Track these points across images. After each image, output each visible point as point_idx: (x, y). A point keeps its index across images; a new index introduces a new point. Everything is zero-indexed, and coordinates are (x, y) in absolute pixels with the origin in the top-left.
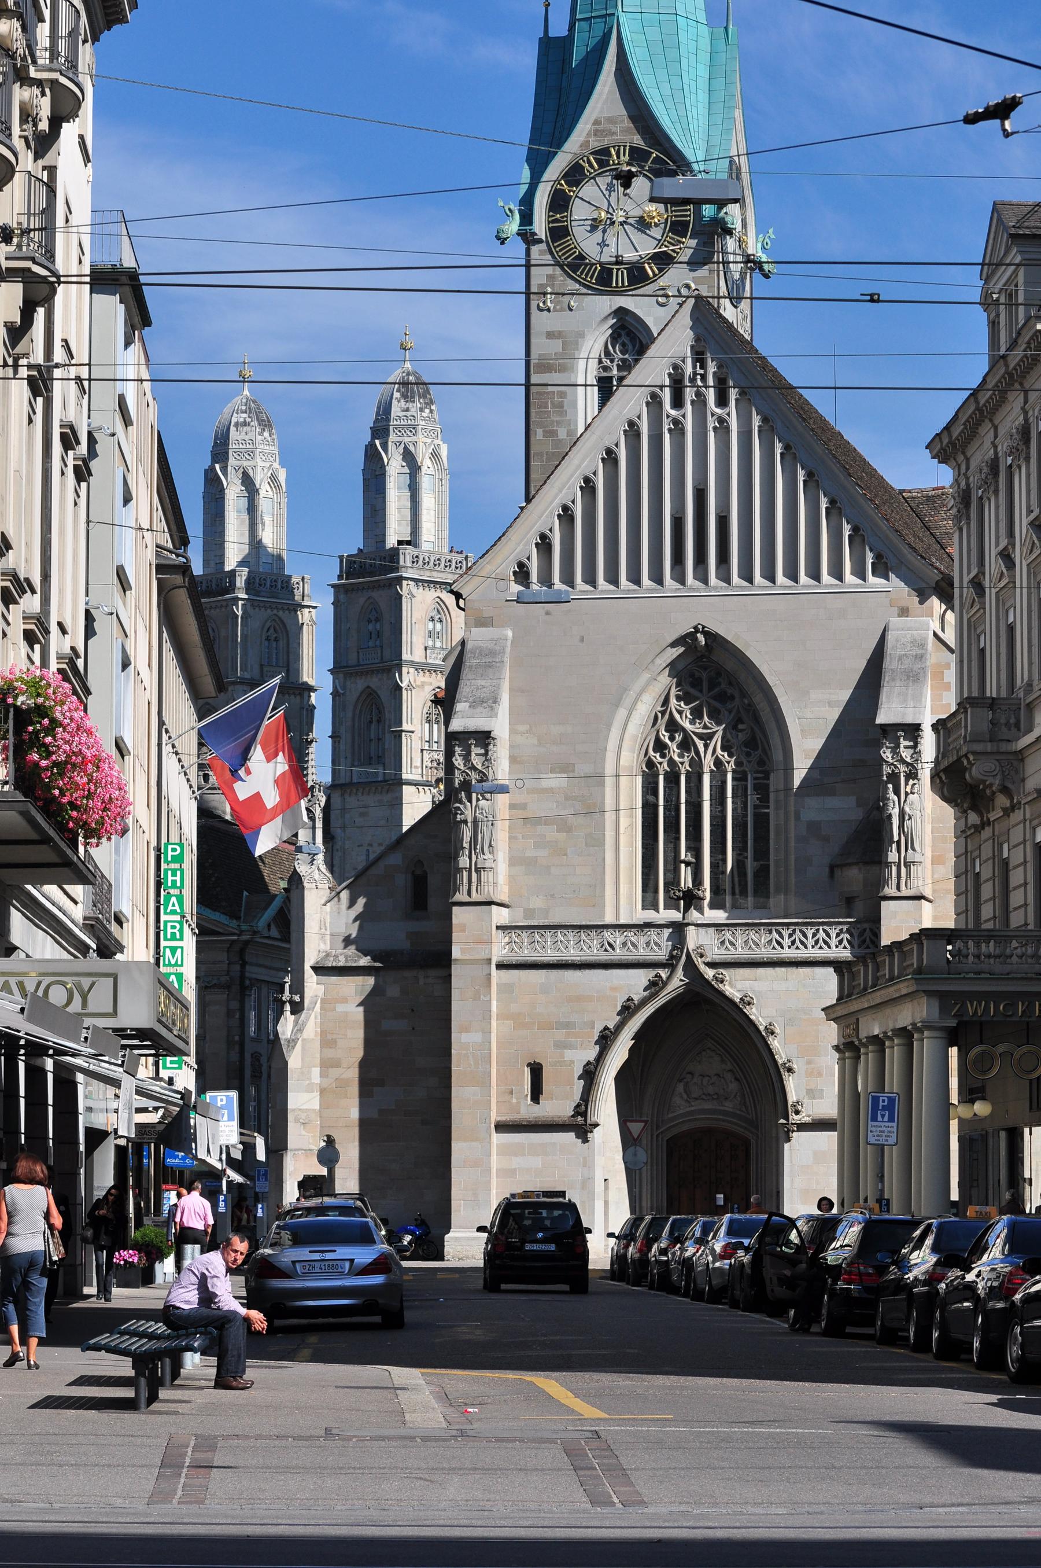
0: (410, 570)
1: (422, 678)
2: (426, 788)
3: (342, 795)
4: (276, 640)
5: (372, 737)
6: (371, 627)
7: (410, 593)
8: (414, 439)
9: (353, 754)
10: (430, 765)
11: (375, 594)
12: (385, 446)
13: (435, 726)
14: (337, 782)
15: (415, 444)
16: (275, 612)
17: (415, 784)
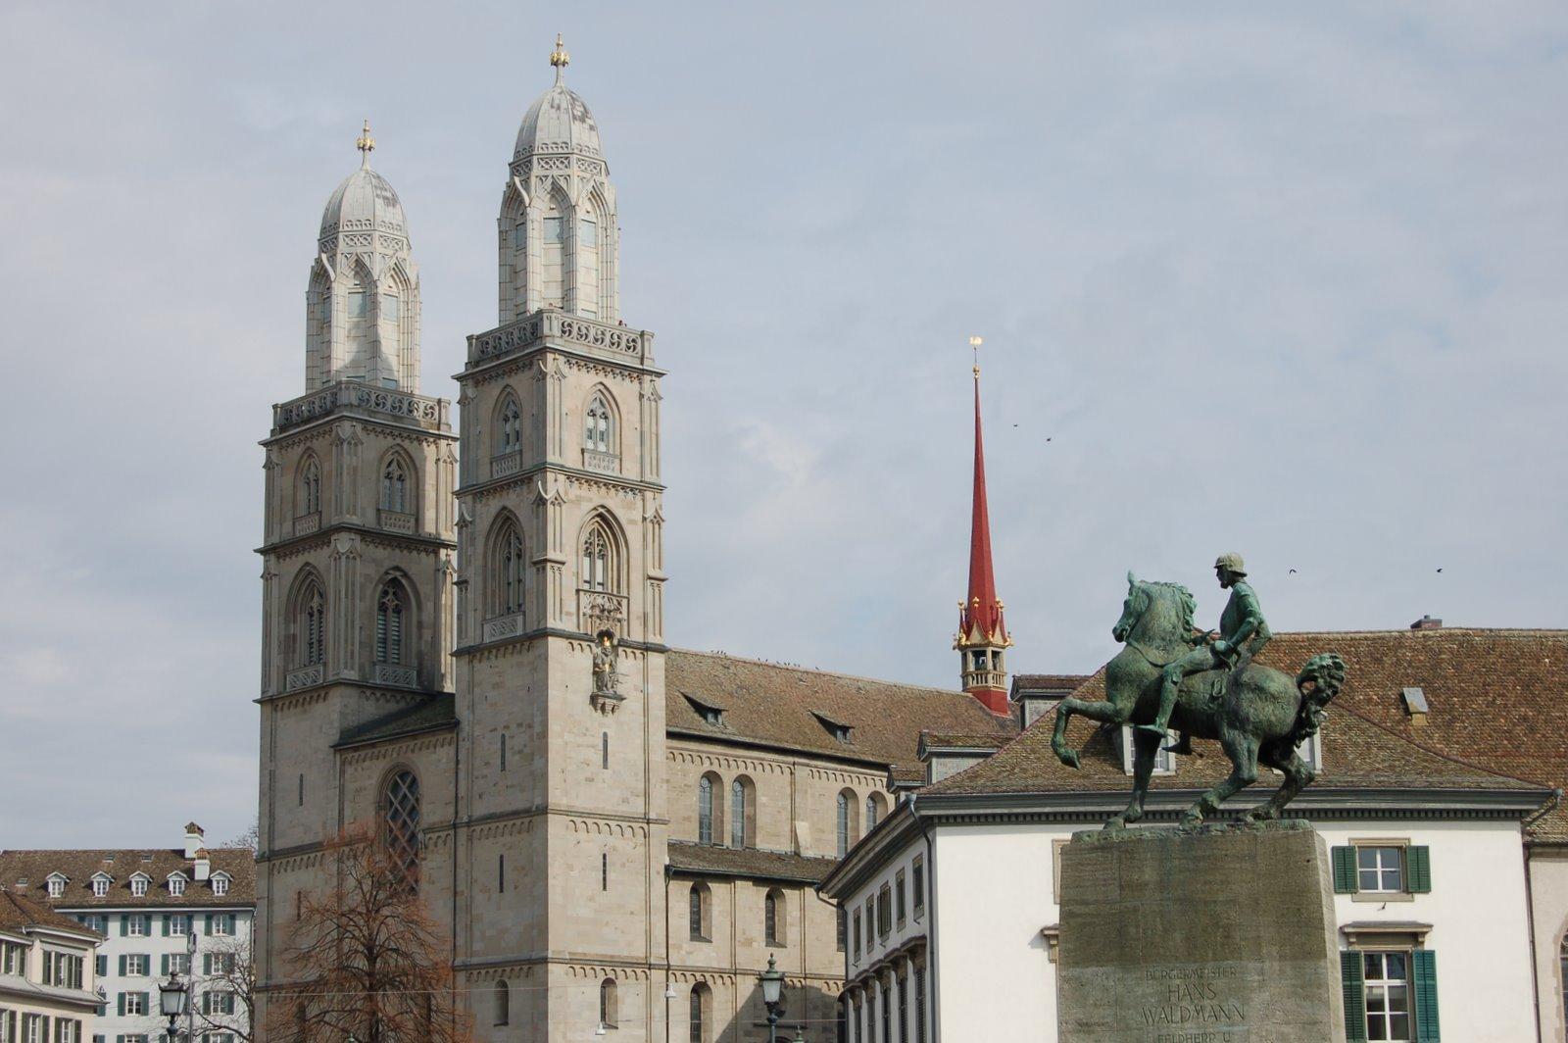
0: (557, 341)
1: (576, 490)
2: (584, 644)
3: (471, 662)
4: (401, 478)
5: (511, 580)
6: (508, 428)
7: (558, 371)
8: (568, 171)
9: (485, 604)
10: (589, 612)
11: (513, 381)
12: (526, 183)
13: (599, 563)
14: (462, 646)
15: (567, 178)
16: (398, 440)
17: (569, 636)
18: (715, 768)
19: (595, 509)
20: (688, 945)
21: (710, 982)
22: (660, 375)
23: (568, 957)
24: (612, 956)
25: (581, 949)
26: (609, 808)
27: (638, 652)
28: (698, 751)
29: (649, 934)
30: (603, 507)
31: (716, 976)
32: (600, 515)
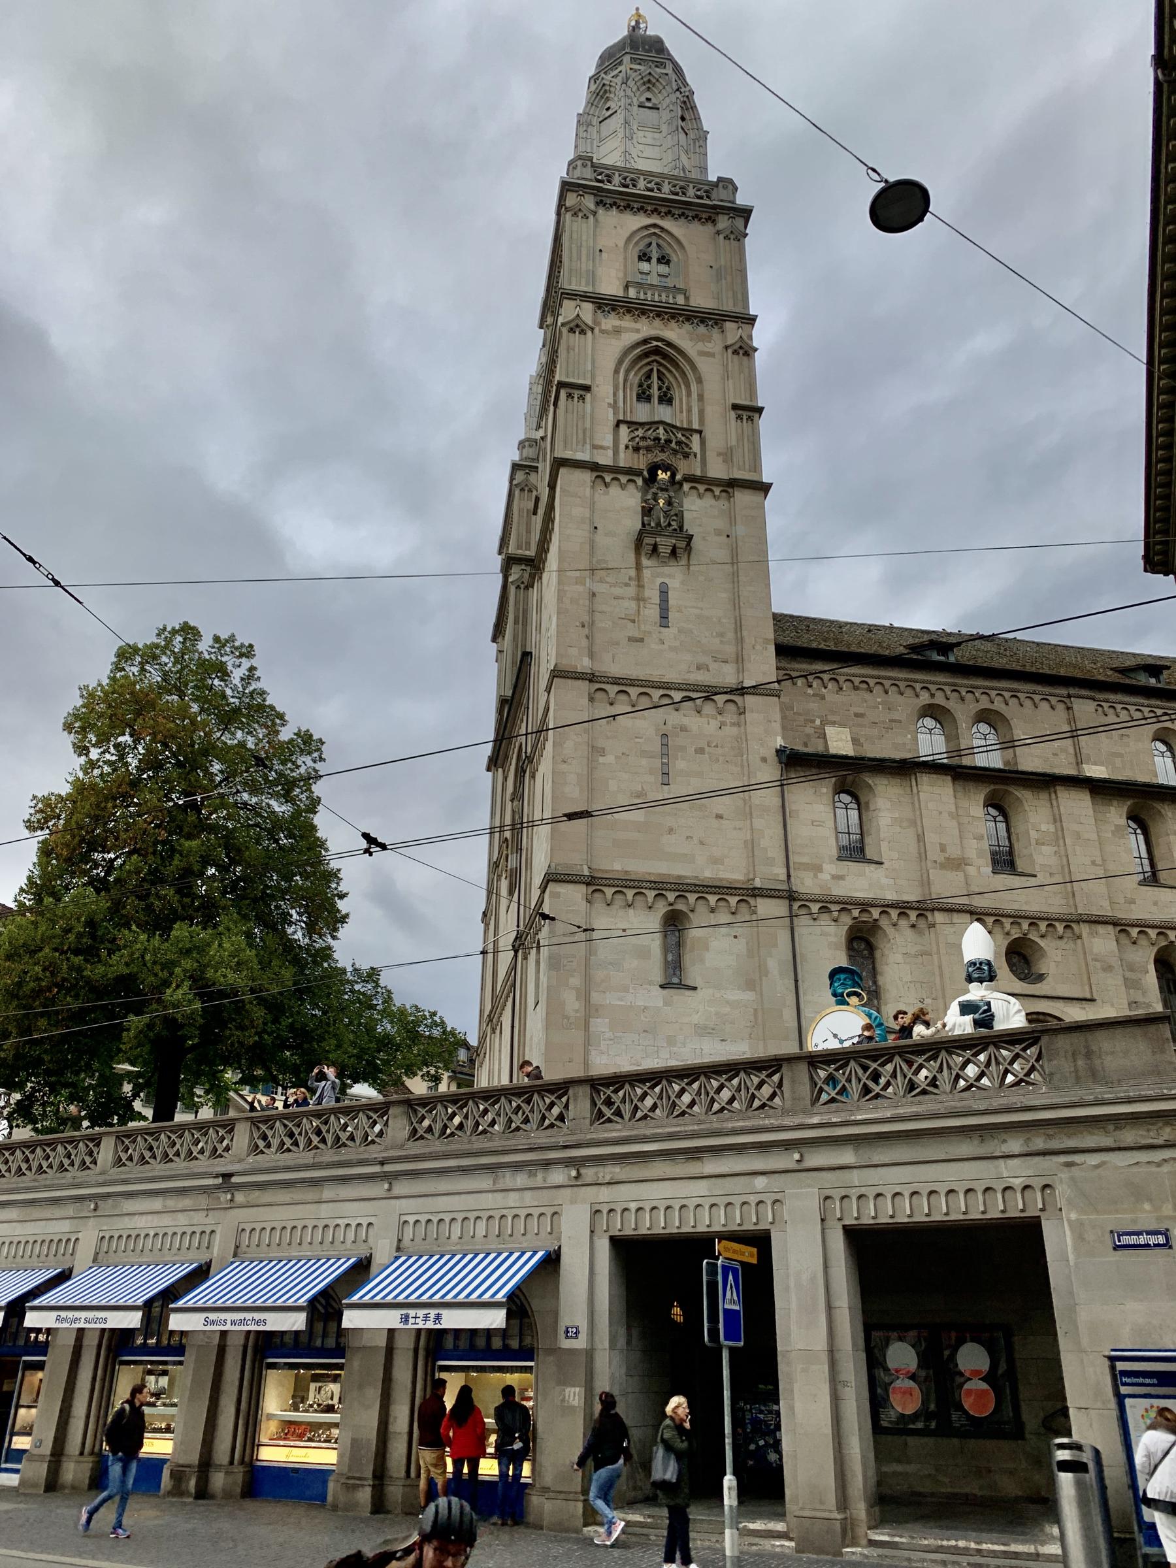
17: (594, 467)
18: (939, 699)
19: (645, 341)
20: (831, 868)
21: (884, 922)
22: (745, 213)
23: (586, 873)
24: (680, 877)
25: (616, 865)
26: (671, 676)
27: (717, 490)
28: (906, 680)
29: (751, 846)
30: (658, 339)
31: (894, 913)
32: (657, 351)
